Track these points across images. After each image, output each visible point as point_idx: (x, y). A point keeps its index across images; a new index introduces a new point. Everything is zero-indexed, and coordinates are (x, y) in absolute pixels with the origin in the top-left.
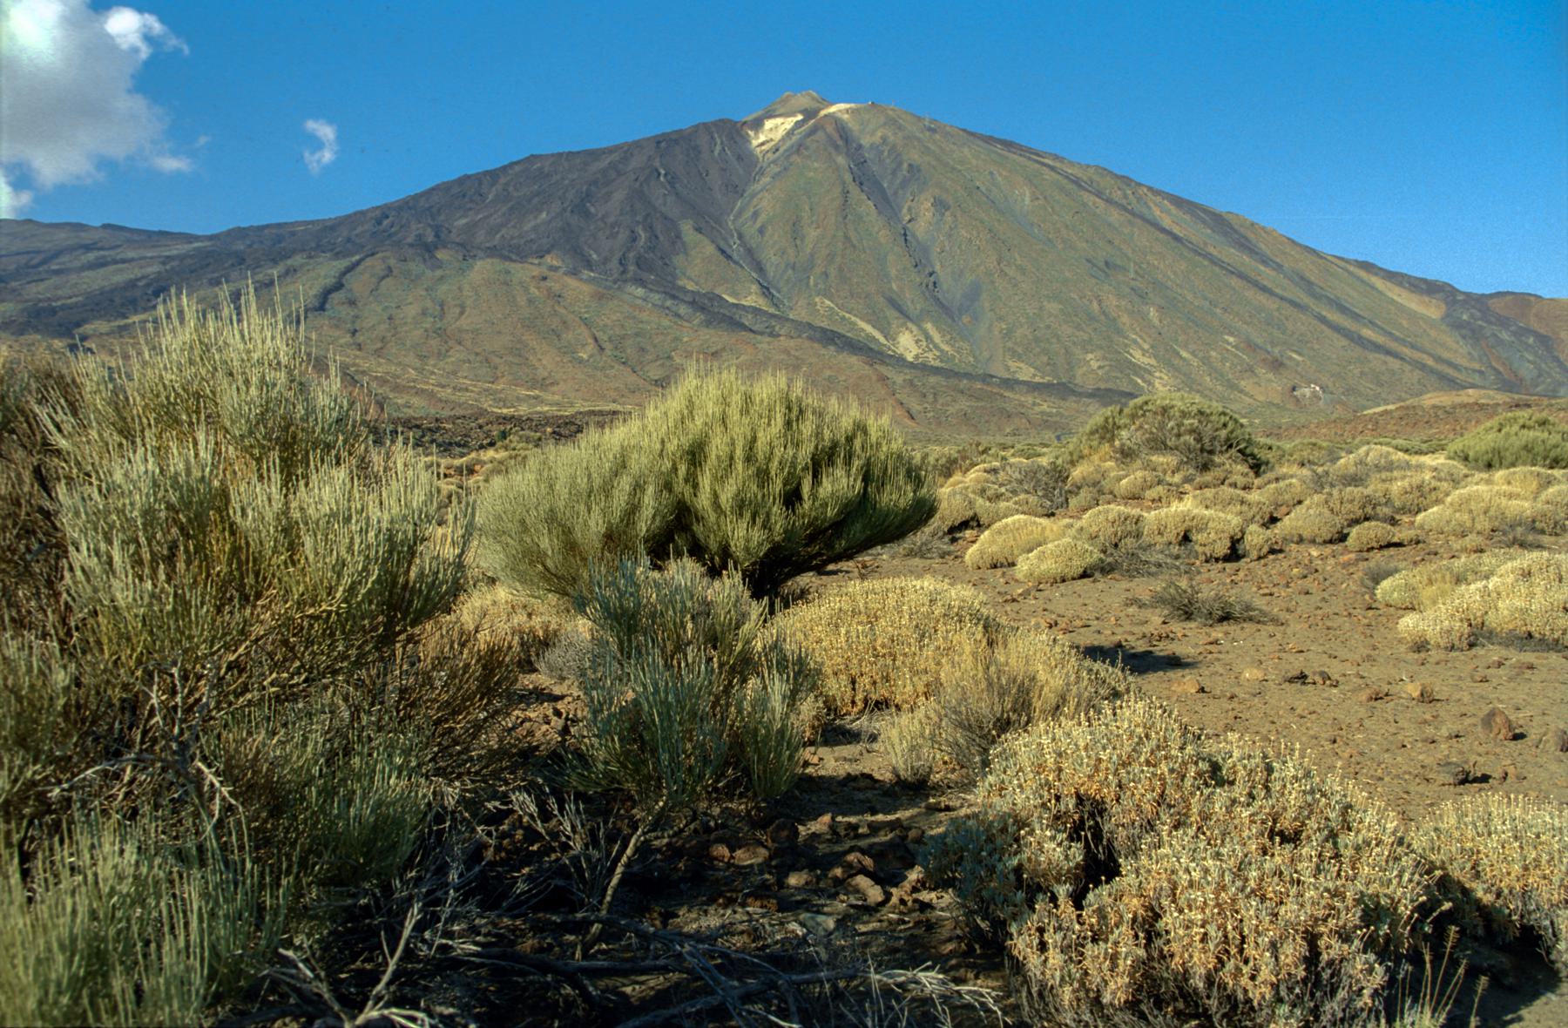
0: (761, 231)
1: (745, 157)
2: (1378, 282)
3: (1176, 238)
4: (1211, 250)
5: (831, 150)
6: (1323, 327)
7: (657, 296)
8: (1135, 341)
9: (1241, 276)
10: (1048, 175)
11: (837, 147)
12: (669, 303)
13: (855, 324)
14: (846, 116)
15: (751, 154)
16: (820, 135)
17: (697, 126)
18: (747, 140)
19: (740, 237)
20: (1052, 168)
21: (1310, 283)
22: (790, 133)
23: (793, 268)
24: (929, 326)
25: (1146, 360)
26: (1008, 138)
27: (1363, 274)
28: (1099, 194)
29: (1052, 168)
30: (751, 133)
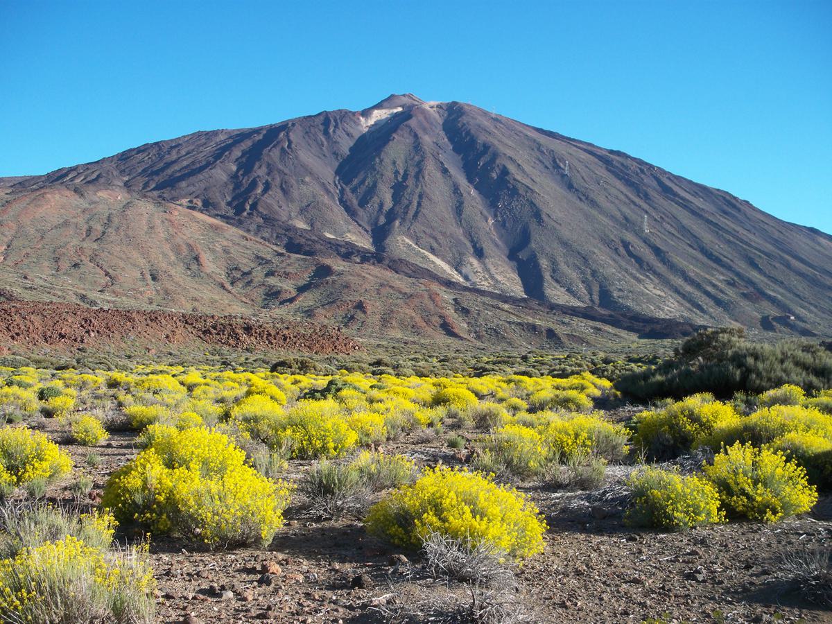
6: (787, 271)
11: (424, 130)
13: (425, 258)
16: (413, 122)
18: (357, 123)
21: (776, 241)
25: (658, 292)
29: (585, 150)
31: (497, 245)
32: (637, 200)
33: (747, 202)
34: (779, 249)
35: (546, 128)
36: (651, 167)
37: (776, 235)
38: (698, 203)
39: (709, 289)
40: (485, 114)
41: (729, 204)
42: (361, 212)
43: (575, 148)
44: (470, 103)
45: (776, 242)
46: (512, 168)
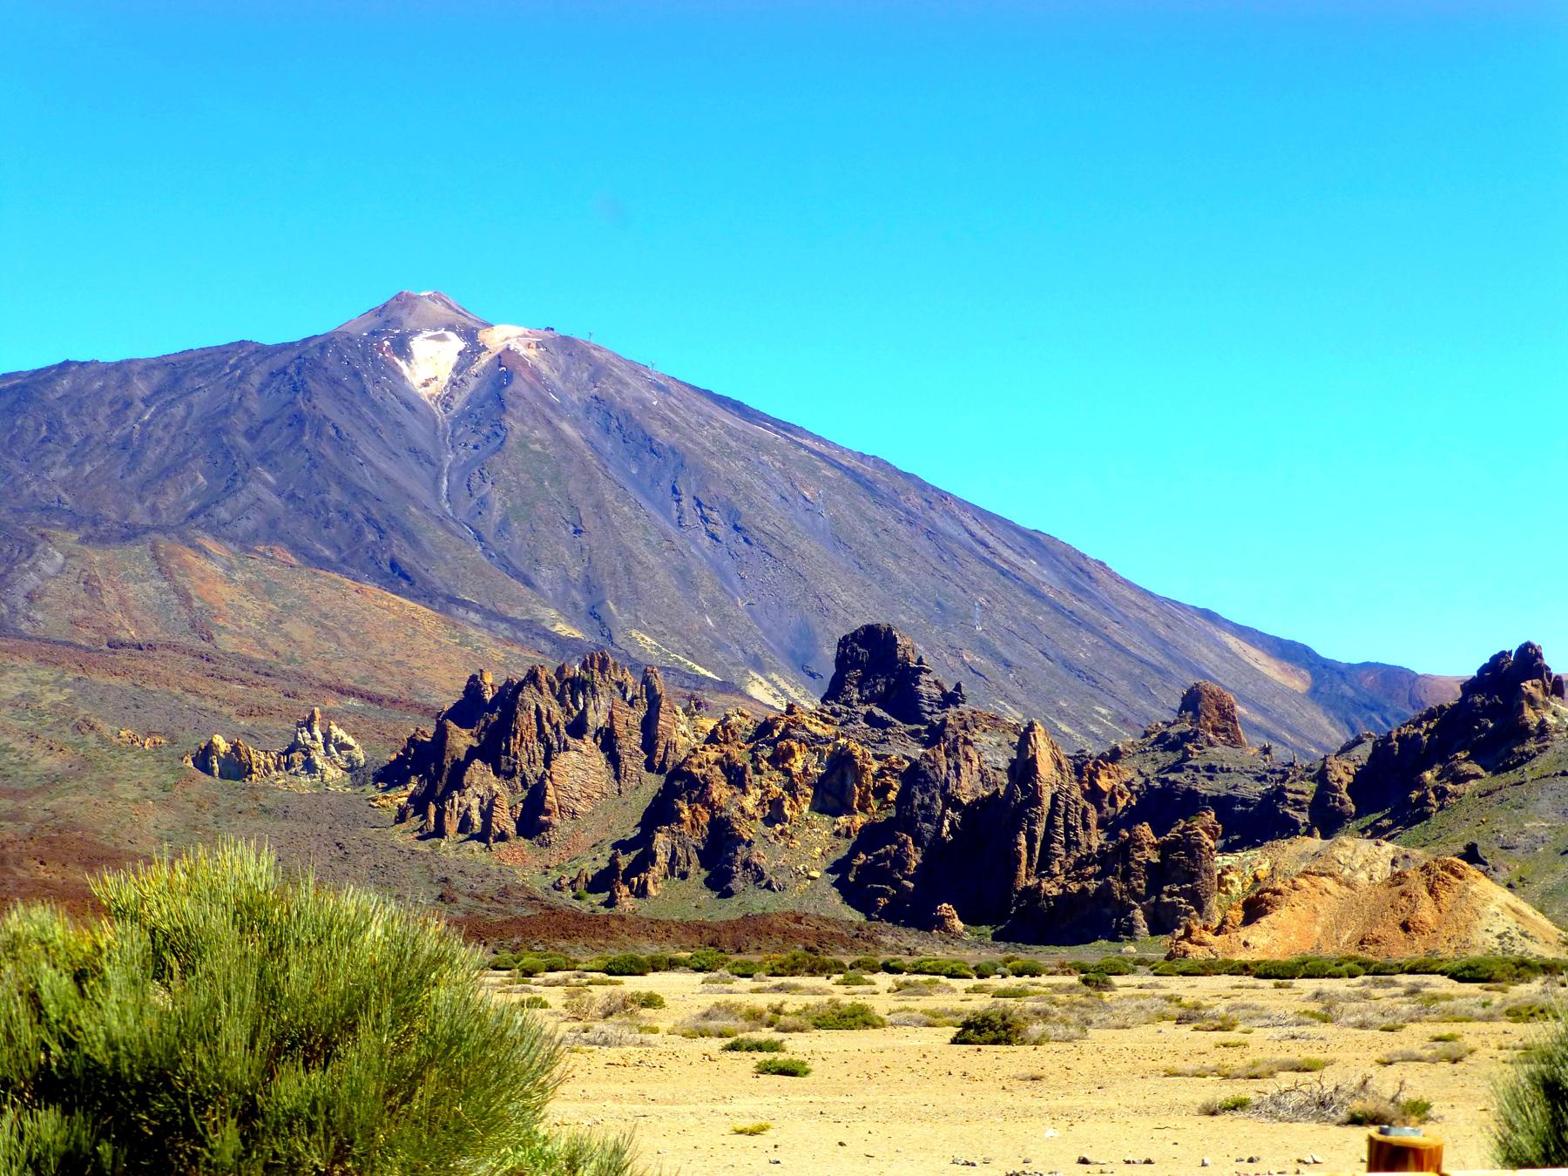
0: (504, 526)
1: (411, 404)
2: (1232, 641)
3: (1003, 573)
4: (1045, 589)
5: (547, 411)
7: (503, 626)
8: (1002, 707)
9: (1091, 629)
10: (828, 472)
12: (520, 635)
14: (531, 354)
15: (417, 397)
16: (518, 386)
17: (324, 343)
19: (480, 538)
20: (821, 456)
21: (1165, 643)
22: (459, 369)
23: (574, 586)
24: (775, 676)
26: (735, 397)
27: (1211, 628)
28: (896, 504)
30: (402, 364)
31: (772, 650)
32: (942, 568)
33: (1102, 564)
34: (1169, 656)
35: (718, 391)
36: (944, 496)
37: (1162, 631)
38: (1031, 568)
39: (1093, 728)
40: (636, 369)
41: (1080, 571)
42: (539, 582)
43: (803, 452)
44: (595, 341)
45: (1164, 645)
46: (744, 509)
